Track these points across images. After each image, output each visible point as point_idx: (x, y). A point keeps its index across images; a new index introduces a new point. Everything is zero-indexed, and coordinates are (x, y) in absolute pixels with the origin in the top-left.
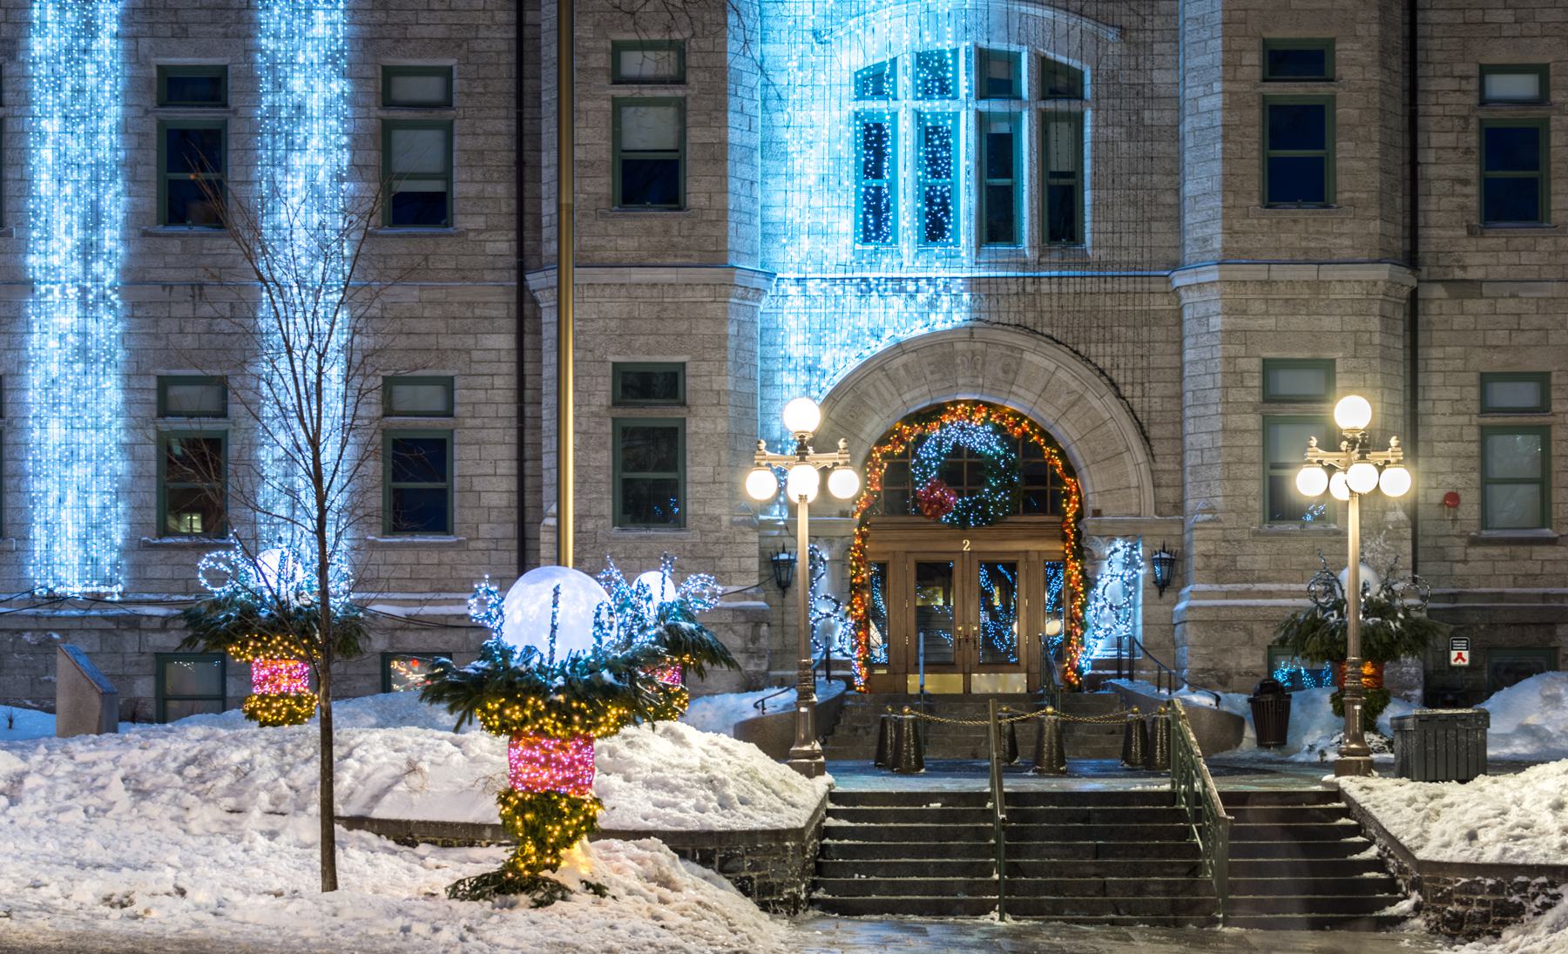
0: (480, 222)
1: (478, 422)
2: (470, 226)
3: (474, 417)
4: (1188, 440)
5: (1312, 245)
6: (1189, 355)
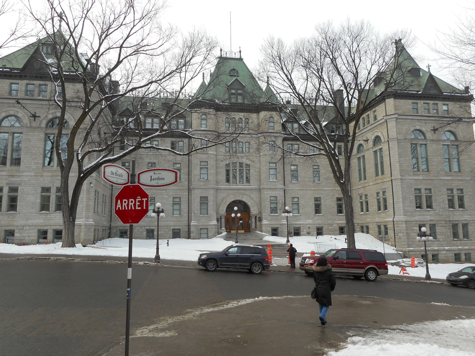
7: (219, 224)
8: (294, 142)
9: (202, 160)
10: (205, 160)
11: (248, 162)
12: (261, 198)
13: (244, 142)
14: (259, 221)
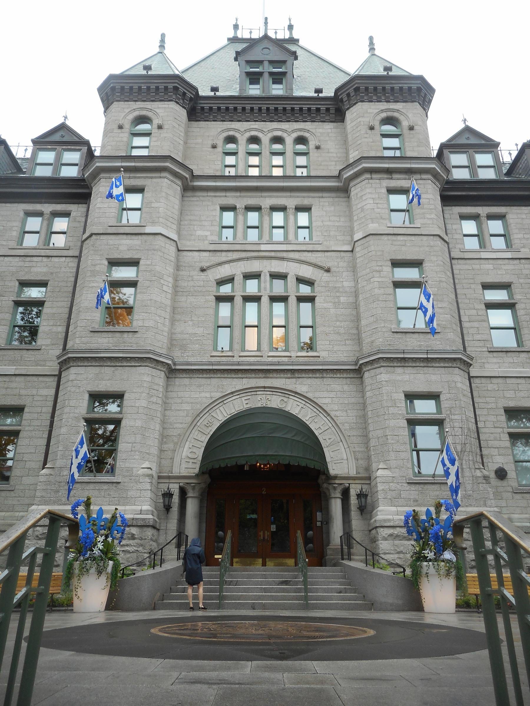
0: (48, 342)
1: (31, 428)
5: (422, 343)
6: (368, 394)
7: (173, 525)
9: (116, 255)
10: (128, 255)
11: (307, 272)
12: (364, 405)
14: (362, 509)
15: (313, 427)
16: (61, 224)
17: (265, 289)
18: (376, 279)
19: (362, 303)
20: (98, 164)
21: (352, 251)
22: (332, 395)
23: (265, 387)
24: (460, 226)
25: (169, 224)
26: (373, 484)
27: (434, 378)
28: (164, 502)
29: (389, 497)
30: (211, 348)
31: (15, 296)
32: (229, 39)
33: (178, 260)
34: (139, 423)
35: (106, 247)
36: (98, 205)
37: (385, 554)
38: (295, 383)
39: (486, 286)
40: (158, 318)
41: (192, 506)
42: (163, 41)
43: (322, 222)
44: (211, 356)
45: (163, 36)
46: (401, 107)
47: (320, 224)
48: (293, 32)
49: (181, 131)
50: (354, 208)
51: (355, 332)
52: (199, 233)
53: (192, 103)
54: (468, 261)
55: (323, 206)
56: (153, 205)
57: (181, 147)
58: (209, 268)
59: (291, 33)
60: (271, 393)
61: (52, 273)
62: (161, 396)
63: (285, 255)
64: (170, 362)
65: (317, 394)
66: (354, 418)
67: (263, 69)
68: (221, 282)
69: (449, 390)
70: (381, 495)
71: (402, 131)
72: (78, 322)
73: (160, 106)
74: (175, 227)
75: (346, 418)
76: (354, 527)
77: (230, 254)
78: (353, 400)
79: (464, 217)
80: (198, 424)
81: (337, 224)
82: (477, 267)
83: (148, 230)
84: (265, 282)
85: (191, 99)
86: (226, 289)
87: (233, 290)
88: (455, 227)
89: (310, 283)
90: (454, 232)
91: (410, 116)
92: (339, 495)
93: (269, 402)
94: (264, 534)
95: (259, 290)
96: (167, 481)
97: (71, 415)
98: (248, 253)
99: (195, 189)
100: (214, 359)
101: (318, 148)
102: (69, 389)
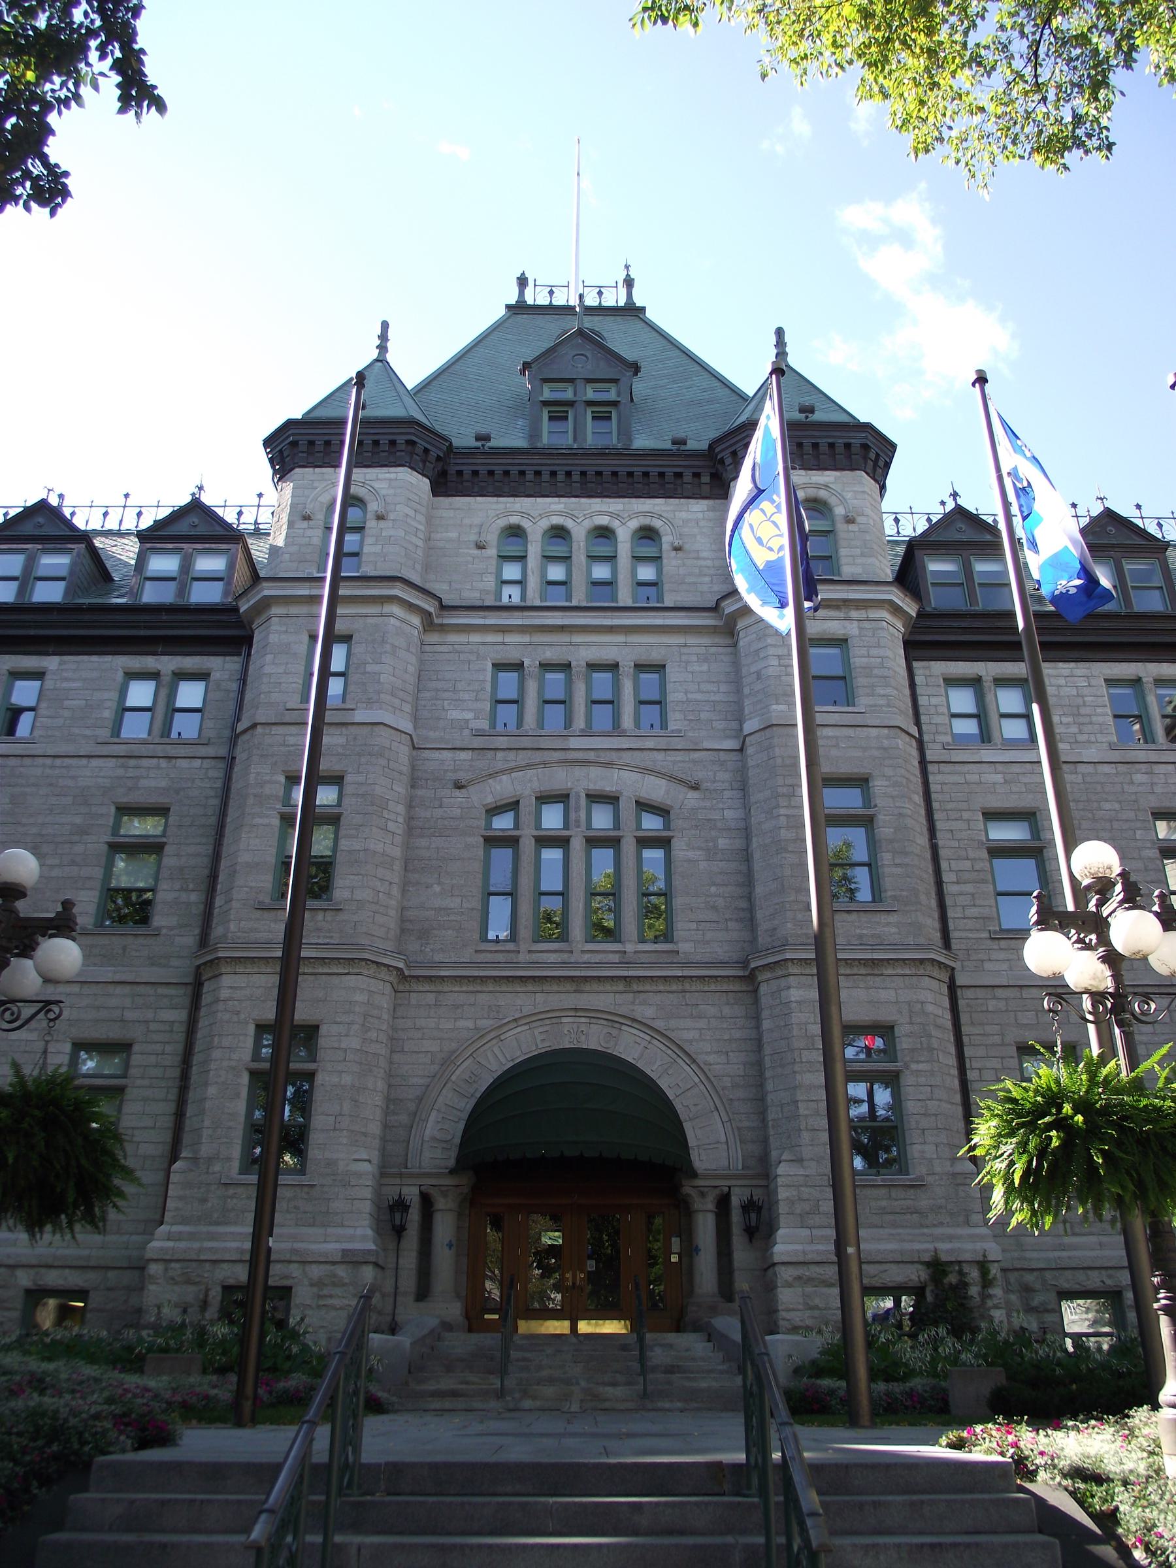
0: (173, 921)
1: (146, 1082)
2: (164, 923)
3: (143, 1078)
4: (769, 1097)
5: (865, 932)
6: (766, 1024)
8: (987, 669)
11: (656, 790)
13: (627, 668)
15: (663, 1084)
16: (190, 694)
17: (578, 821)
18: (782, 811)
19: (757, 855)
20: (266, 593)
21: (741, 750)
22: (702, 1024)
23: (576, 1010)
24: (944, 699)
25: (397, 702)
26: (772, 1186)
27: (884, 995)
28: (392, 1220)
29: (798, 1211)
30: (476, 936)
31: (109, 833)
32: (508, 307)
33: (413, 768)
34: (347, 1079)
35: (282, 748)
36: (268, 669)
37: (788, 1310)
38: (633, 1003)
39: (992, 816)
40: (379, 883)
41: (445, 1228)
42: (384, 337)
43: (686, 693)
44: (476, 951)
45: (385, 326)
46: (832, 479)
47: (680, 696)
48: (635, 292)
49: (420, 523)
50: (744, 671)
51: (744, 904)
52: (455, 714)
53: (441, 464)
54: (958, 767)
55: (687, 662)
56: (369, 668)
57: (420, 552)
58: (471, 782)
59: (629, 295)
60: (587, 1020)
61: (177, 792)
62: (384, 1028)
63: (613, 757)
64: (401, 965)
65: (673, 1023)
66: (741, 1067)
67: (575, 395)
68: (495, 810)
69: (911, 1017)
70: (783, 1208)
71: (833, 524)
72: (234, 891)
73: (380, 476)
74: (407, 708)
75: (727, 1066)
76: (736, 1264)
77: (511, 755)
78: (737, 1034)
79: (952, 682)
80: (453, 1078)
81: (713, 698)
82: (975, 778)
83: (359, 716)
84: (577, 809)
85: (439, 458)
86: (504, 823)
87: (517, 826)
88: (934, 701)
89: (662, 811)
90: (933, 711)
91: (849, 496)
92: (711, 1206)
93: (583, 1037)
94: (574, 1276)
95: (567, 826)
96: (398, 1181)
97: (225, 1064)
98: (546, 752)
99: (443, 629)
100: (481, 958)
101: (677, 549)
102: (219, 1014)
